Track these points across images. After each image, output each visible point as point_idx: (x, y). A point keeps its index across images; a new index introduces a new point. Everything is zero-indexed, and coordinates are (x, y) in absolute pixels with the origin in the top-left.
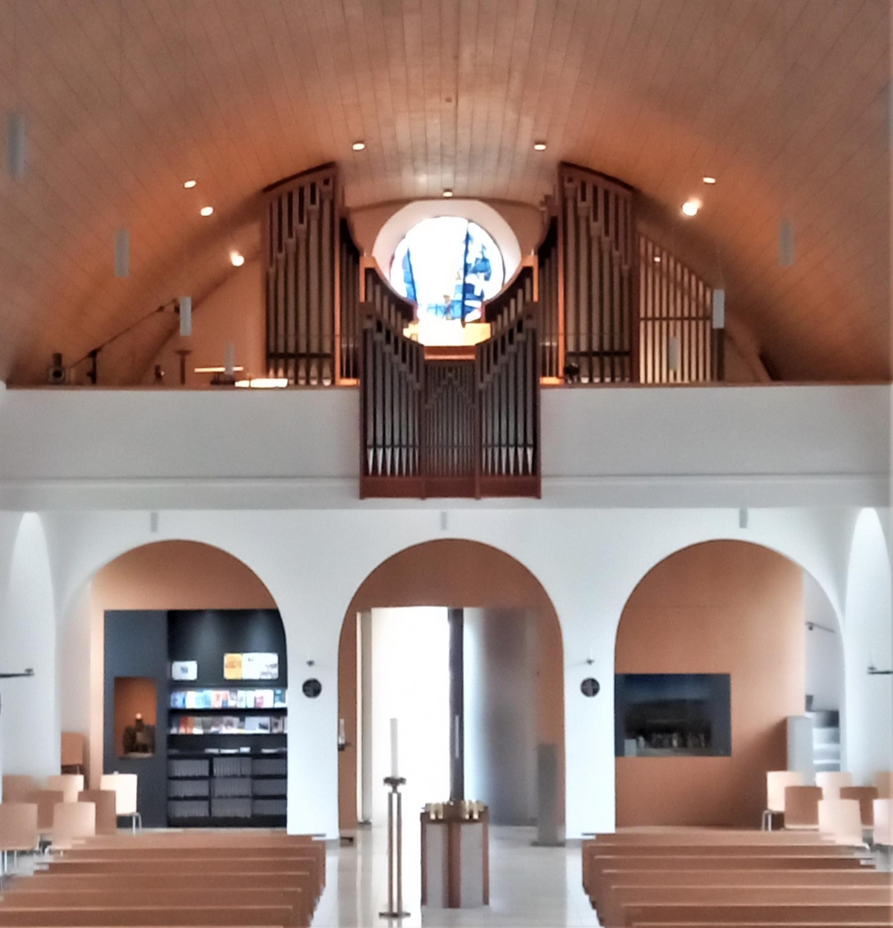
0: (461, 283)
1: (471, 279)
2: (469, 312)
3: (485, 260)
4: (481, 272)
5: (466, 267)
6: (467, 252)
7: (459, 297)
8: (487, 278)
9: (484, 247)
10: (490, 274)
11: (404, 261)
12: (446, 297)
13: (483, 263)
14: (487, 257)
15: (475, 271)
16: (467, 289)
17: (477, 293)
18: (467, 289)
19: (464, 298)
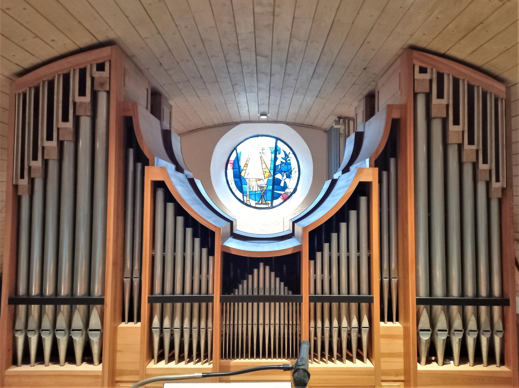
0: (271, 178)
1: (278, 176)
2: (277, 198)
3: (288, 164)
4: (285, 172)
5: (275, 166)
6: (276, 159)
7: (270, 187)
8: (289, 176)
9: (286, 155)
10: (291, 173)
11: (234, 164)
12: (261, 187)
13: (286, 166)
14: (288, 161)
15: (281, 172)
16: (276, 182)
17: (282, 184)
18: (276, 182)
19: (273, 189)
